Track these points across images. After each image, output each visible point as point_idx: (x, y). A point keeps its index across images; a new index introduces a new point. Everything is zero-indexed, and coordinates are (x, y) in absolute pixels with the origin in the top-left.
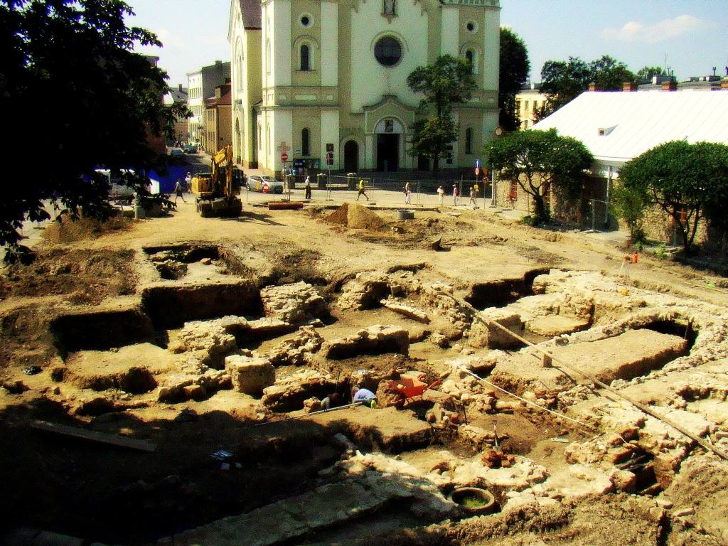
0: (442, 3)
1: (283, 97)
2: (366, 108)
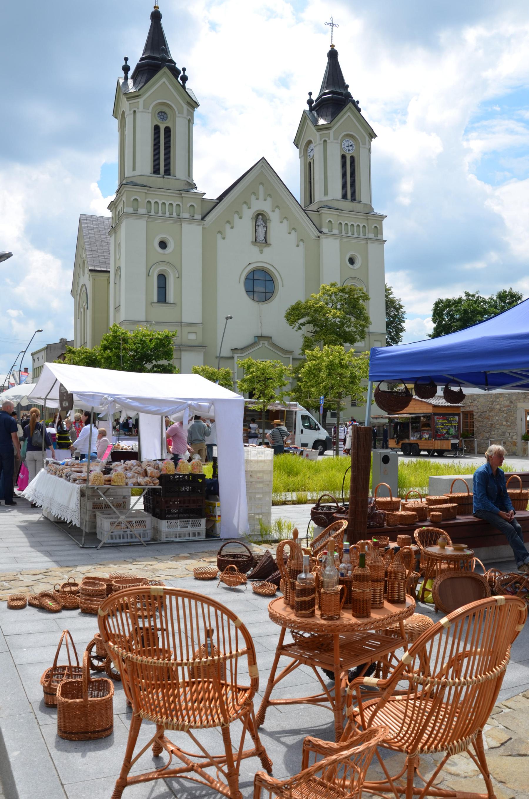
0: (321, 232)
2: (234, 350)
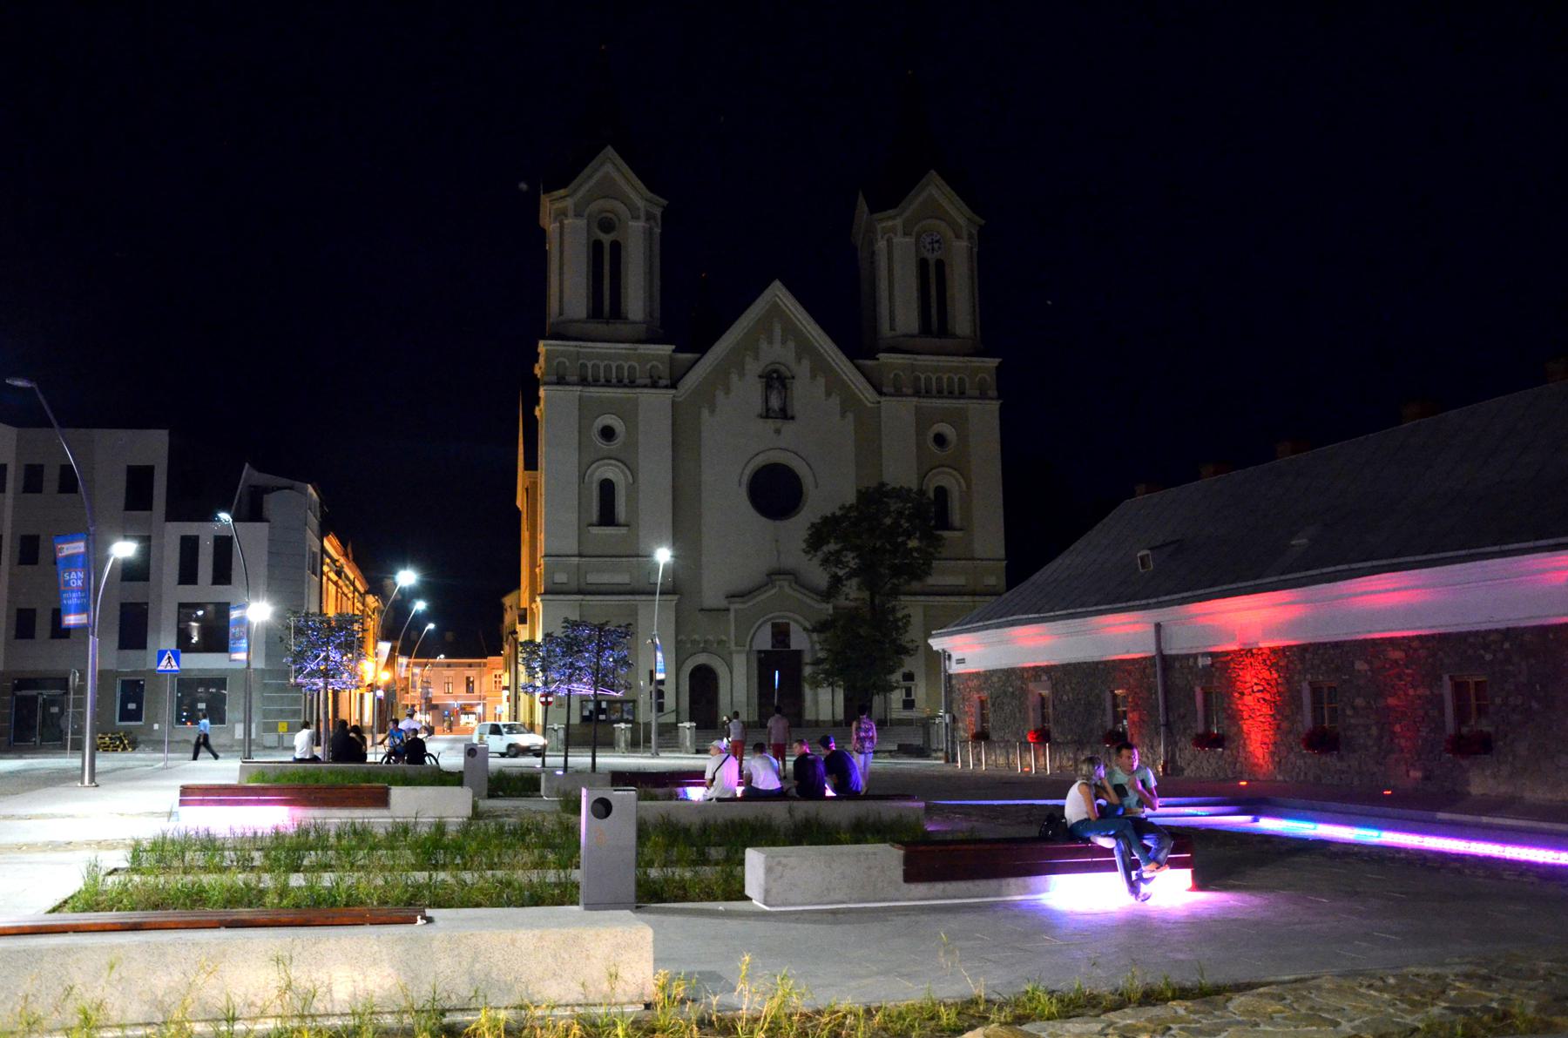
0: (881, 393)
1: (561, 578)
2: (732, 596)
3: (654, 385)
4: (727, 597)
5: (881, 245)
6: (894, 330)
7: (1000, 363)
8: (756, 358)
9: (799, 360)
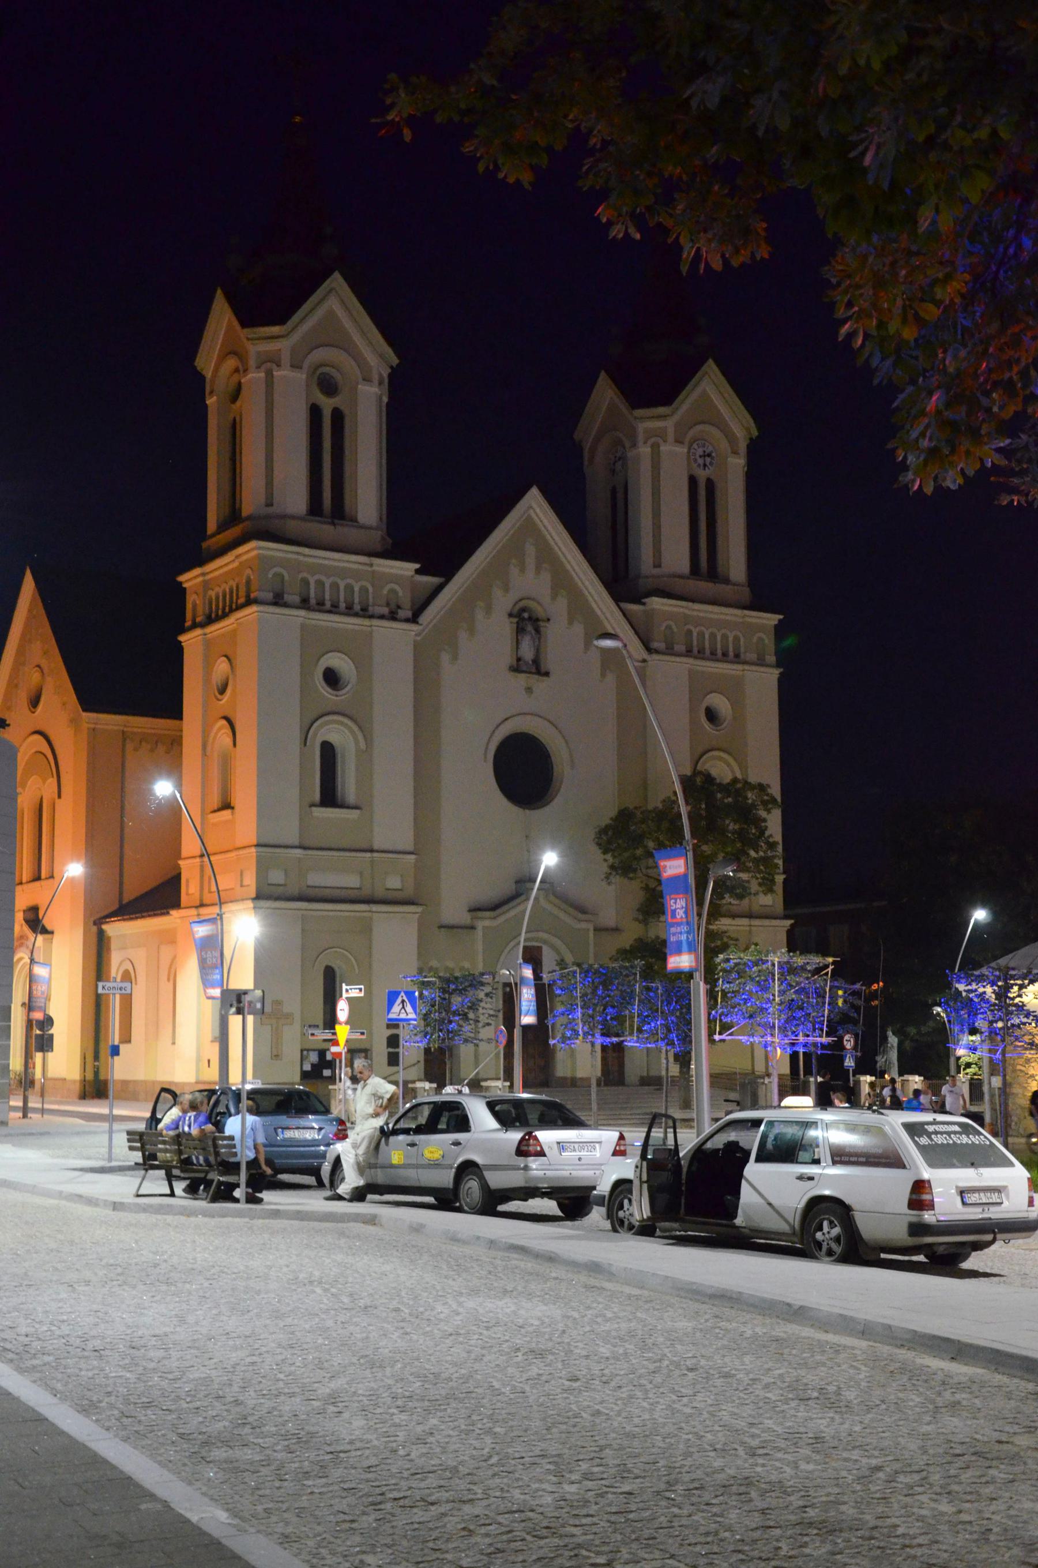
0: (649, 650)
1: (276, 876)
2: (475, 909)
3: (393, 617)
4: (470, 911)
5: (645, 450)
6: (659, 566)
7: (780, 621)
8: (506, 589)
9: (554, 597)
